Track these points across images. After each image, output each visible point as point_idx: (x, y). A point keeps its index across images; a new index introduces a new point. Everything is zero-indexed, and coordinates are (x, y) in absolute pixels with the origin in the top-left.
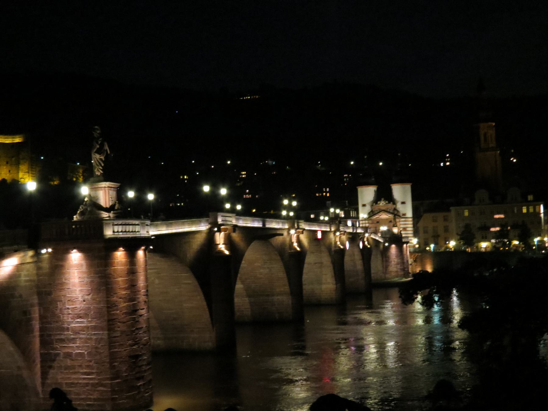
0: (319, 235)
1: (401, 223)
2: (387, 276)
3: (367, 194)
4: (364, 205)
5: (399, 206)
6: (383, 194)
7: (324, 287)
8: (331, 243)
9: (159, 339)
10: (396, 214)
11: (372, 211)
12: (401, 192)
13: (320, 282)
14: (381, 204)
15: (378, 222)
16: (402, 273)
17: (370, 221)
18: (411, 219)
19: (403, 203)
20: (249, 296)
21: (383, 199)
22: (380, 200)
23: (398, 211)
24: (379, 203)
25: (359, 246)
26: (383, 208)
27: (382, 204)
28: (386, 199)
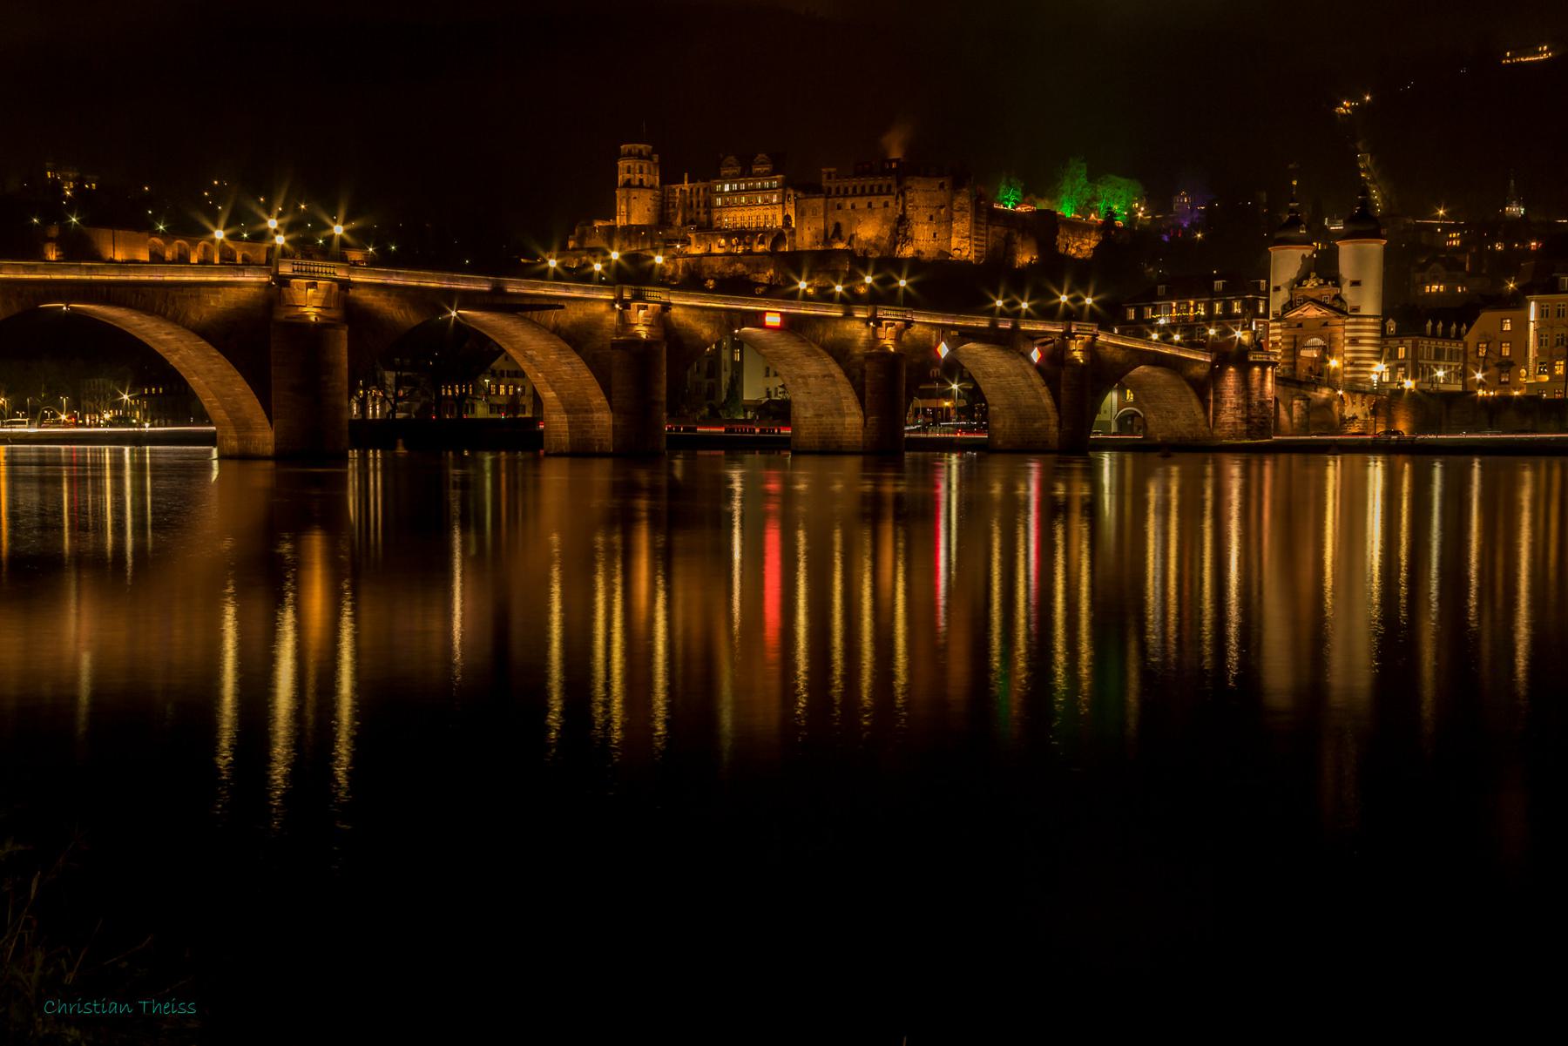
0: (773, 320)
2: (1217, 432)
3: (1287, 263)
5: (1347, 291)
7: (848, 420)
8: (853, 340)
10: (1339, 308)
11: (1291, 302)
13: (840, 412)
15: (1300, 325)
16: (1244, 427)
19: (1356, 283)
20: (567, 412)
21: (1313, 274)
22: (1307, 277)
23: (1342, 300)
25: (1030, 360)
28: (1319, 276)
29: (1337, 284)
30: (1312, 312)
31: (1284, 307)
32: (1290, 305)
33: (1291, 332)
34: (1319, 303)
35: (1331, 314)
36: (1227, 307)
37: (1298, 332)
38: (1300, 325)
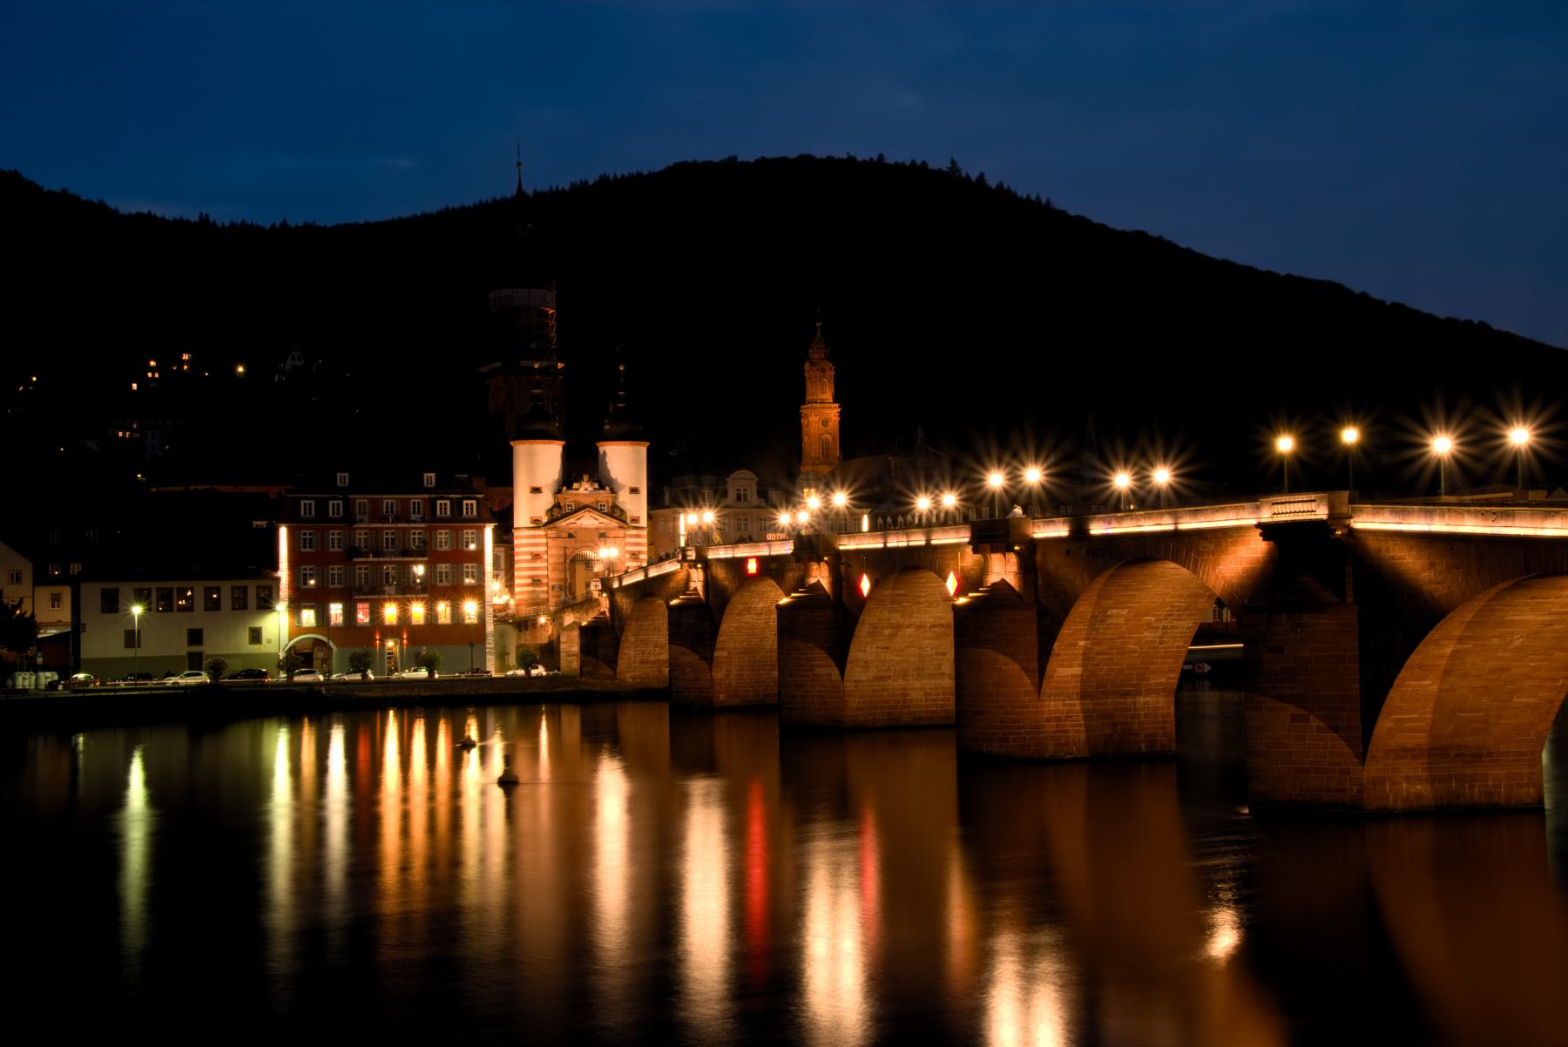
1: (629, 540)
4: (536, 490)
6: (582, 464)
9: (1419, 780)
11: (557, 506)
12: (625, 462)
14: (582, 491)
15: (570, 536)
17: (551, 533)
18: (645, 533)
19: (634, 491)
20: (1083, 696)
21: (586, 477)
22: (579, 480)
24: (575, 485)
26: (586, 501)
27: (584, 489)
28: (593, 479)
29: (613, 491)
30: (588, 521)
31: (550, 511)
32: (557, 513)
33: (561, 542)
34: (595, 508)
35: (614, 523)
36: (457, 505)
37: (570, 543)
38: (570, 536)
